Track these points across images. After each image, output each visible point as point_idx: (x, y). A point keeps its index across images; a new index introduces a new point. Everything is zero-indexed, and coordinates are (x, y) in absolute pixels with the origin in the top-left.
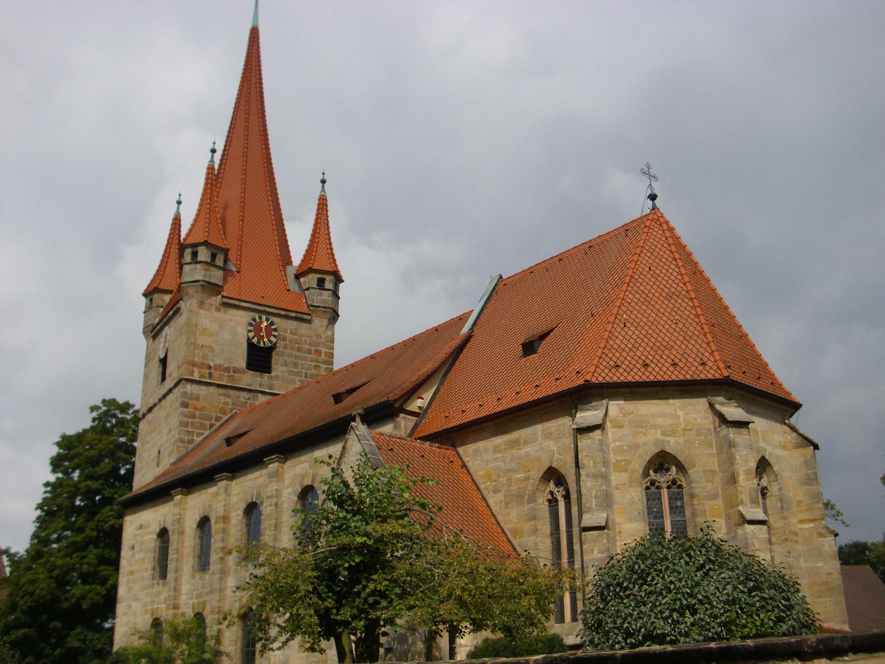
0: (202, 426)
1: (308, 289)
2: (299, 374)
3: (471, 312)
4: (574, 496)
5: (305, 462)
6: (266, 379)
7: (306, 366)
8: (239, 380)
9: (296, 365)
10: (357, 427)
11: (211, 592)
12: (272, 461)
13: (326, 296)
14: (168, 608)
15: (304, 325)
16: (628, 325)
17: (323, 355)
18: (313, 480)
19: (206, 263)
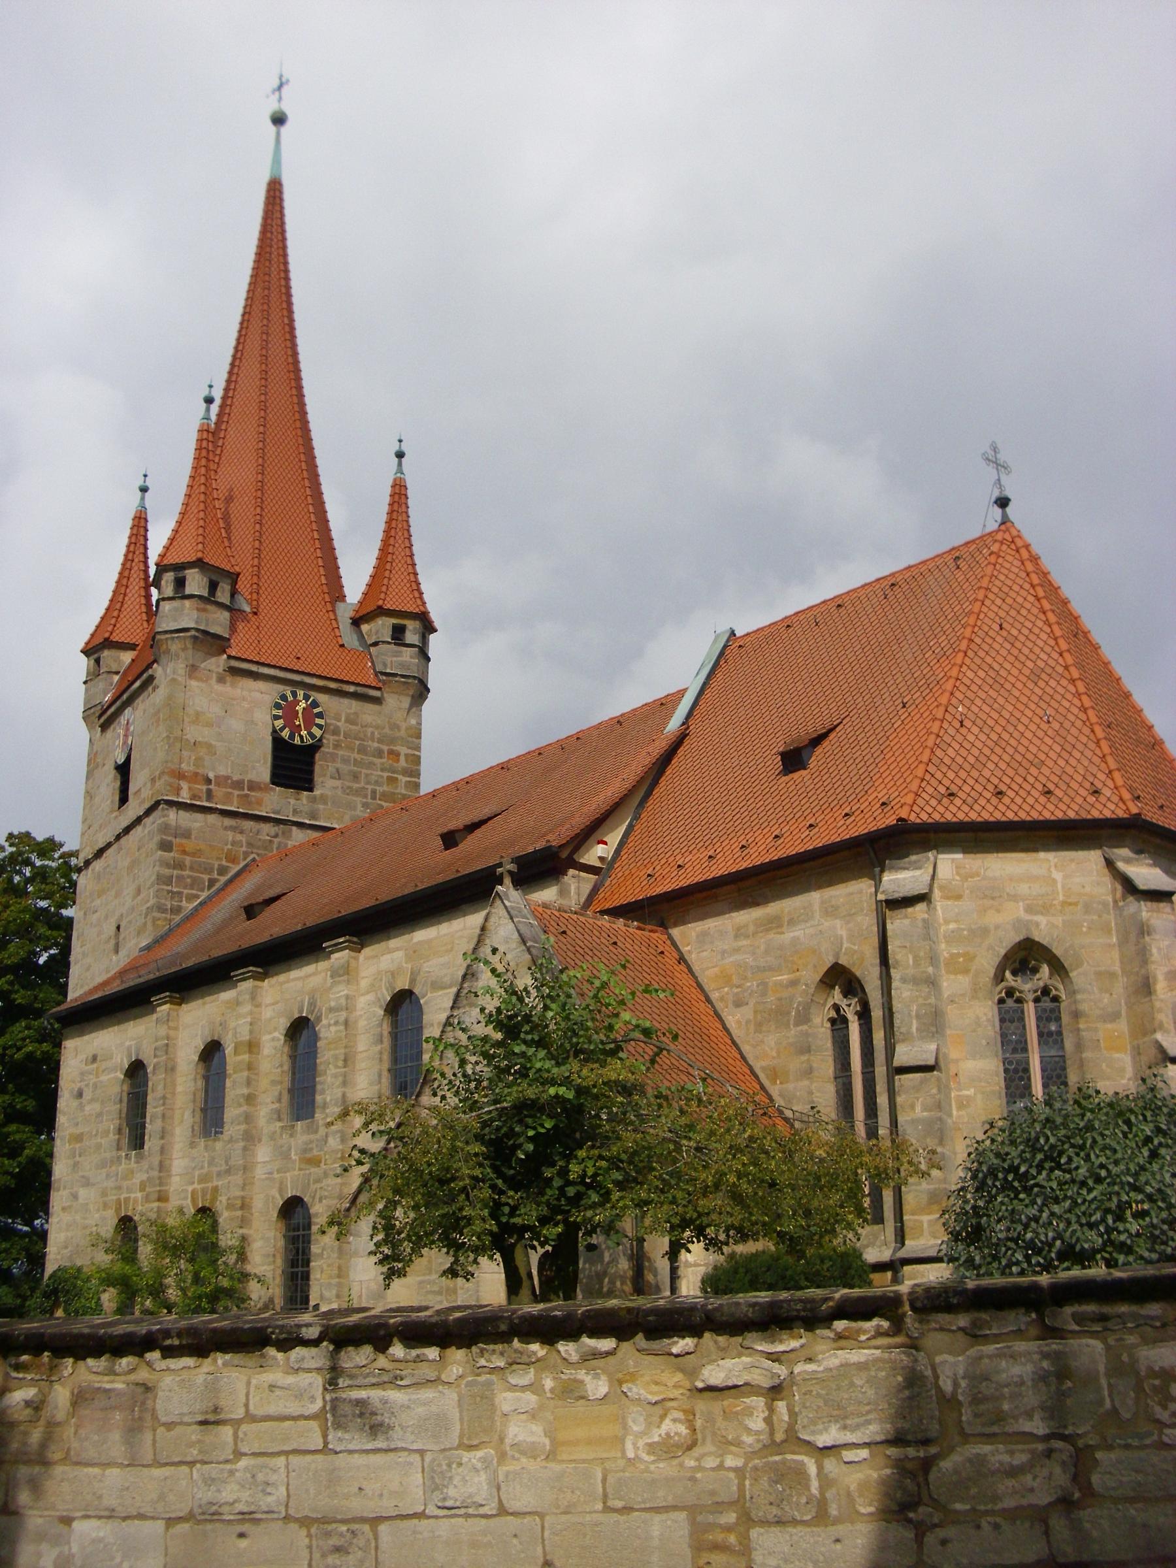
0: (195, 884)
1: (375, 644)
2: (359, 792)
3: (682, 693)
4: (877, 1014)
5: (398, 949)
6: (305, 802)
7: (374, 778)
8: (259, 803)
9: (356, 777)
10: (506, 894)
11: (228, 1172)
12: (337, 948)
13: (408, 656)
14: (147, 1199)
15: (370, 707)
16: (967, 723)
17: (402, 758)
18: (413, 981)
19: (200, 597)
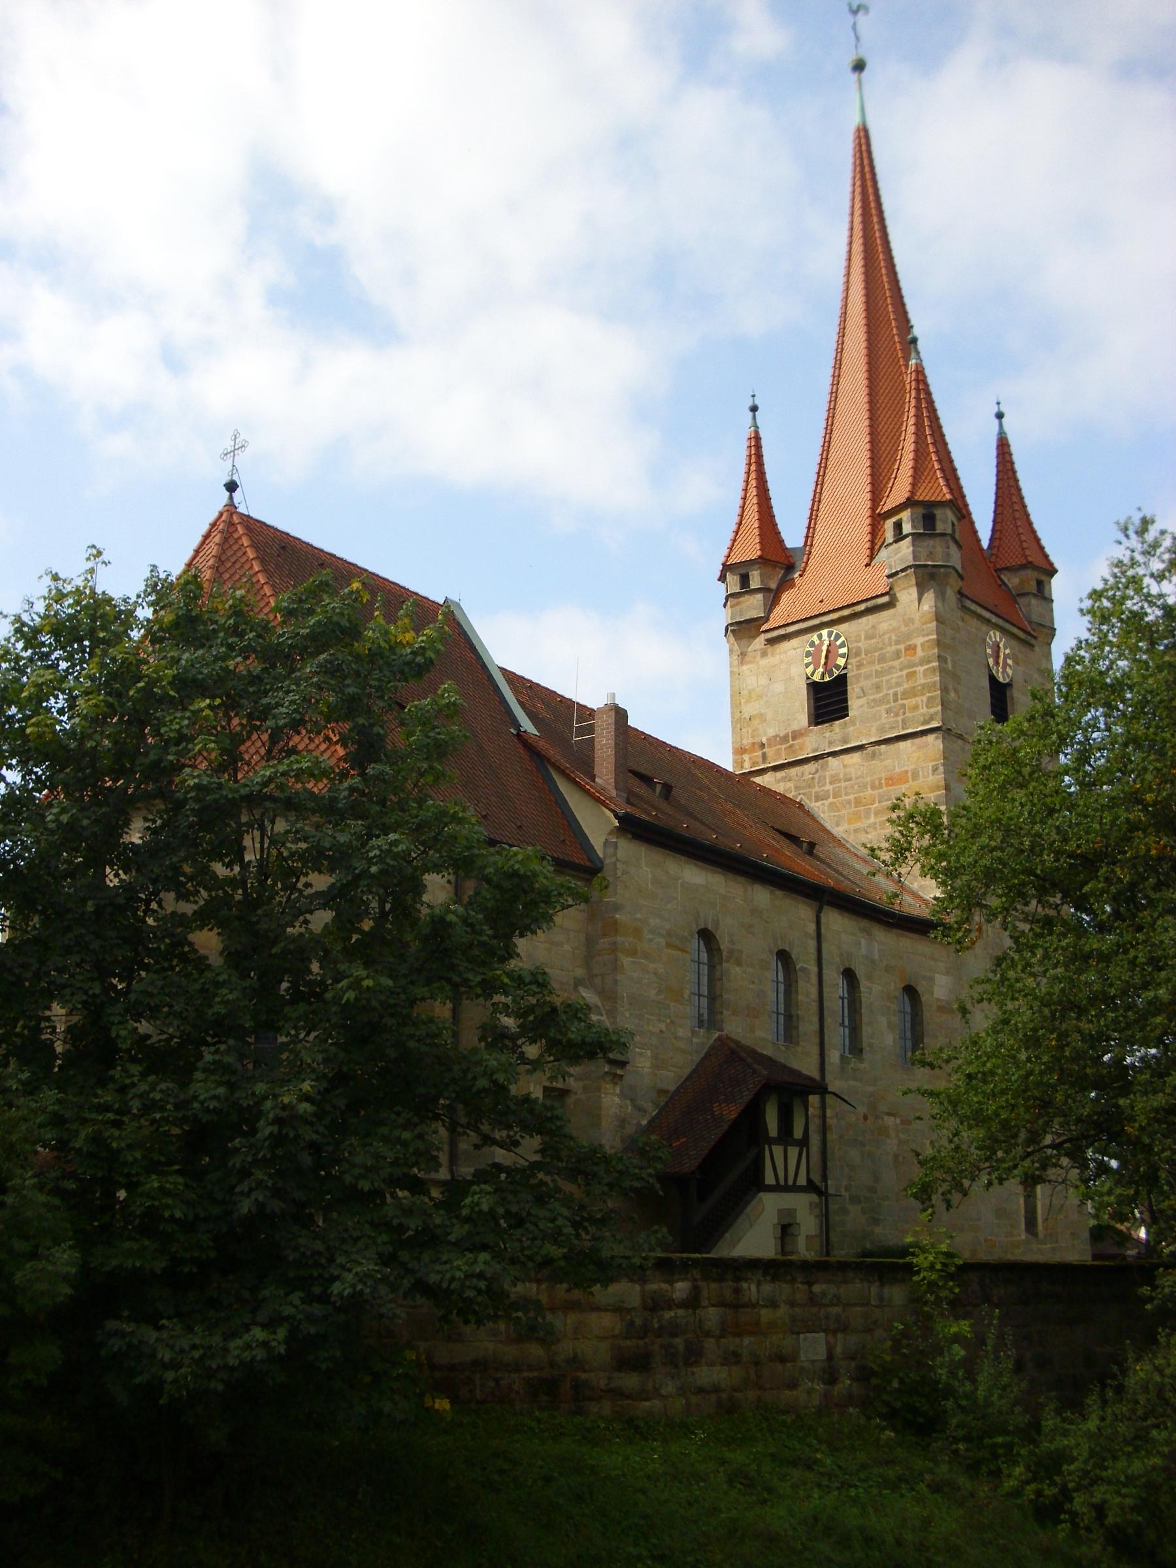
2: (881, 702)
6: (837, 730)
17: (919, 649)
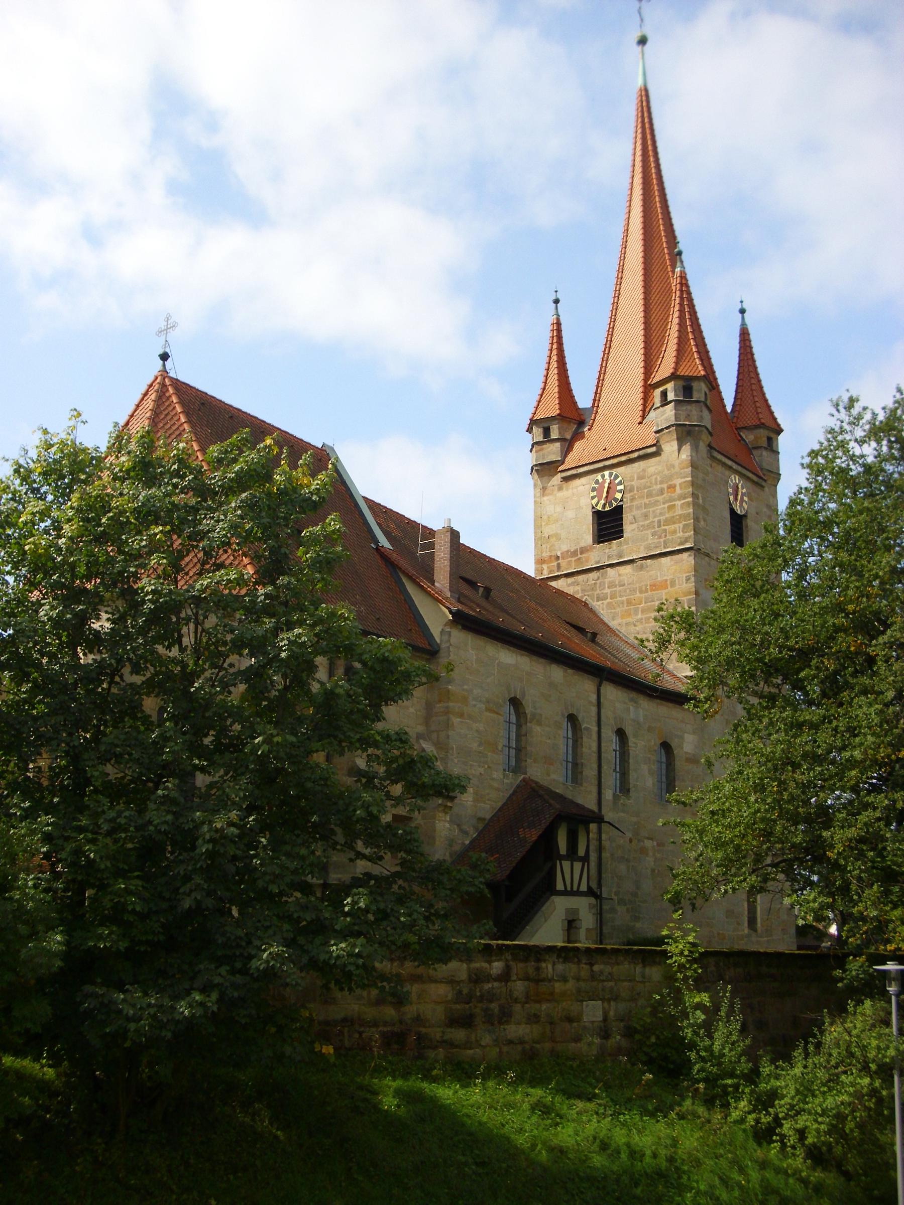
2: (648, 527)
6: (615, 548)
7: (658, 511)
17: (678, 488)
